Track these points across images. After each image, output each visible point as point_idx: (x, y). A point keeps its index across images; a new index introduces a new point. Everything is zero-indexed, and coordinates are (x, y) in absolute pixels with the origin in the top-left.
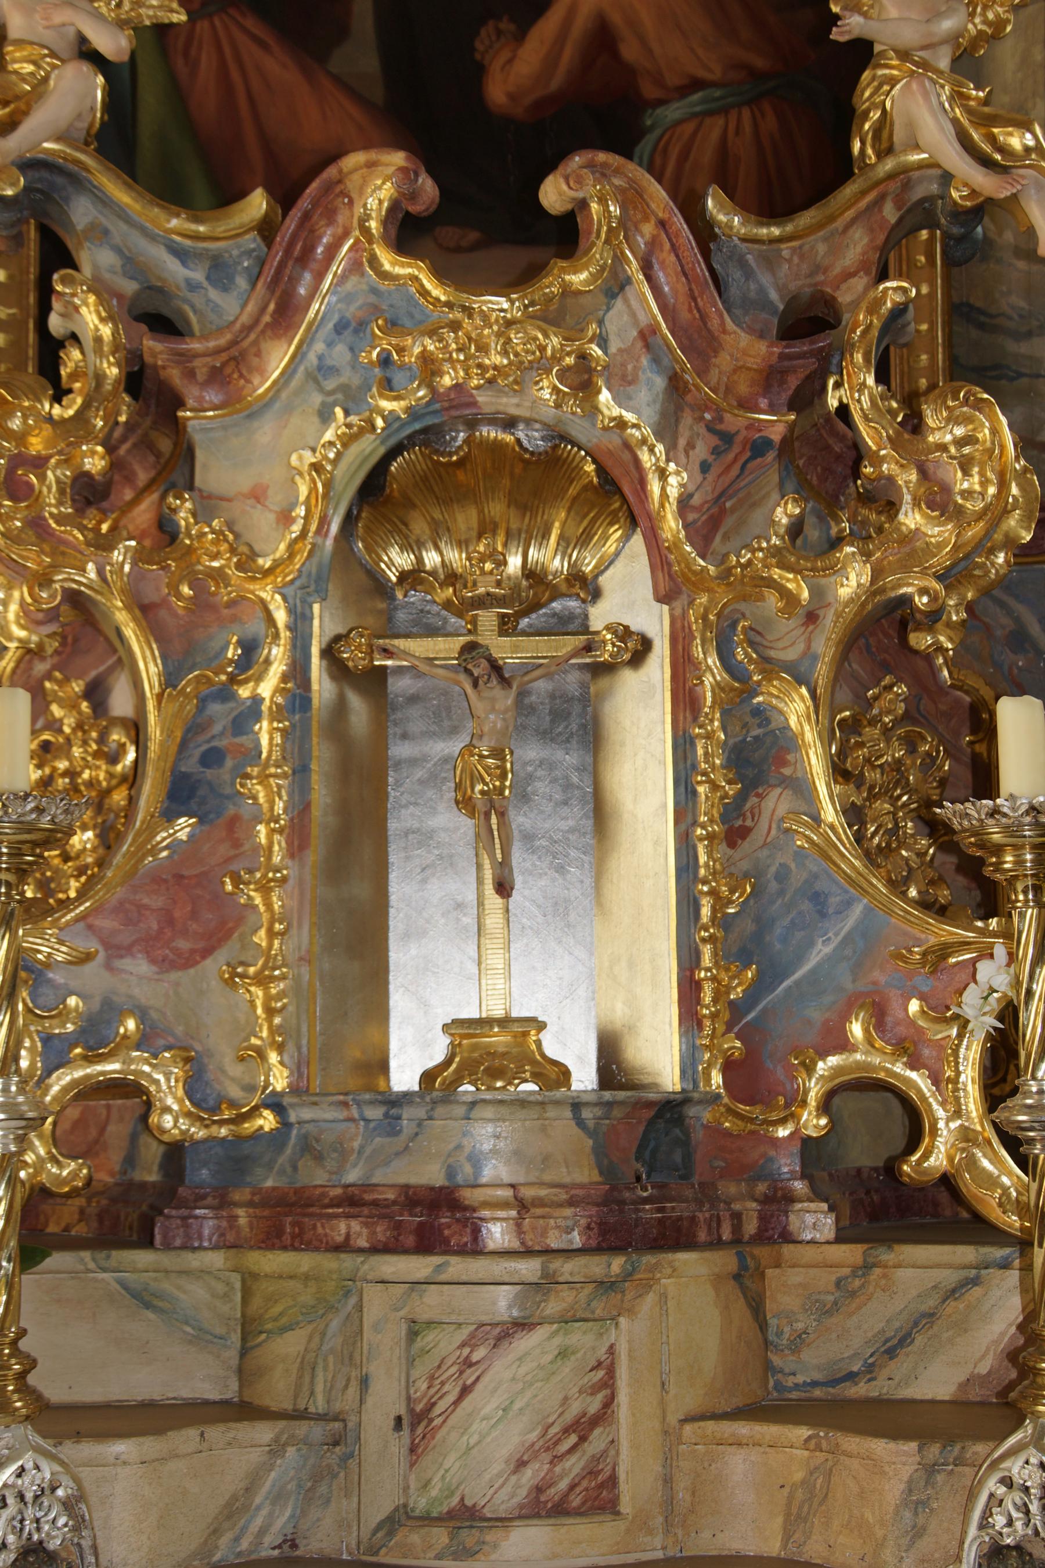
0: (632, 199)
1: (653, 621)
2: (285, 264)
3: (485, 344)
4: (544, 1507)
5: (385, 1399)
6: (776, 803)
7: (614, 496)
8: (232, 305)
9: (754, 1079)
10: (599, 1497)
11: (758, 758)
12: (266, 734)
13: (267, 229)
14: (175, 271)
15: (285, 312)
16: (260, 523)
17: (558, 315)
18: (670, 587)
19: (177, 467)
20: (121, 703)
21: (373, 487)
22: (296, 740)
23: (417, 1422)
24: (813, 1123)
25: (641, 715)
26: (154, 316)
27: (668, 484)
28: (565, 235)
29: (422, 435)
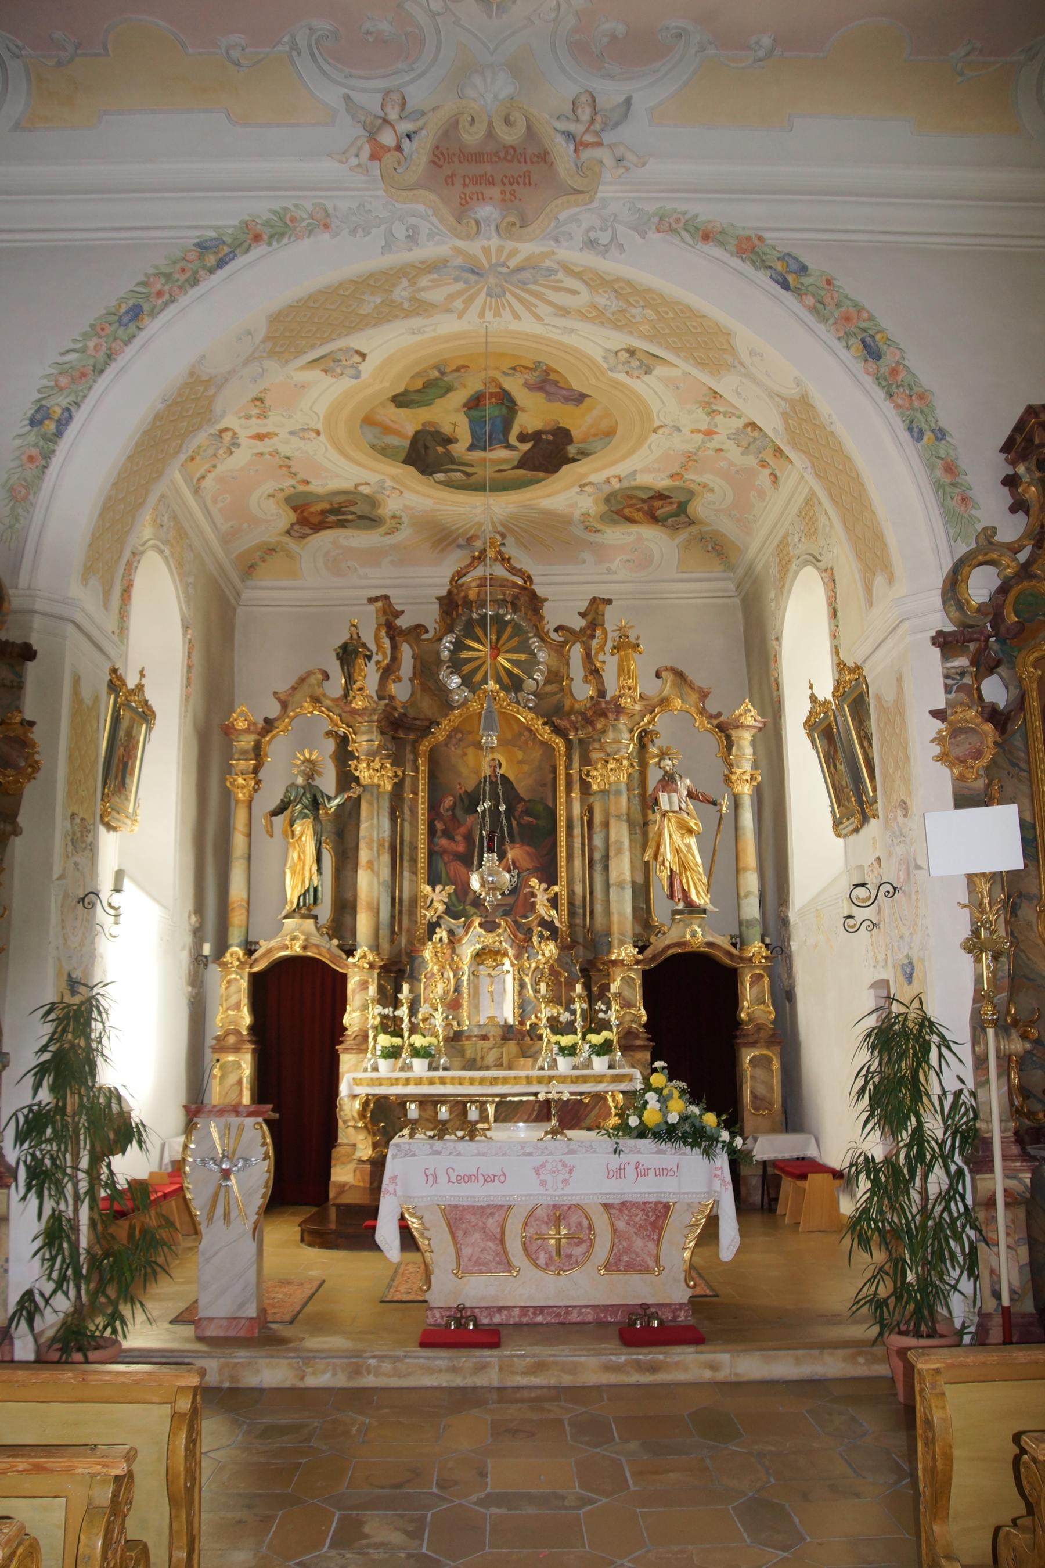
0: (506, 922)
1: (511, 969)
2: (467, 927)
3: (489, 939)
4: (496, 1066)
5: (479, 1056)
6: (525, 991)
7: (505, 954)
8: (461, 931)
9: (522, 1023)
10: (501, 1065)
11: (522, 985)
12: (465, 983)
13: (465, 922)
14: (453, 927)
15: (467, 933)
16: (464, 958)
17: (499, 935)
18: (513, 965)
19: (454, 951)
20: (445, 976)
21: (477, 954)
22: (469, 984)
23: (482, 1058)
24: (528, 1027)
25: (509, 978)
26: (451, 932)
27: (511, 952)
28: (499, 926)
29: (483, 948)
